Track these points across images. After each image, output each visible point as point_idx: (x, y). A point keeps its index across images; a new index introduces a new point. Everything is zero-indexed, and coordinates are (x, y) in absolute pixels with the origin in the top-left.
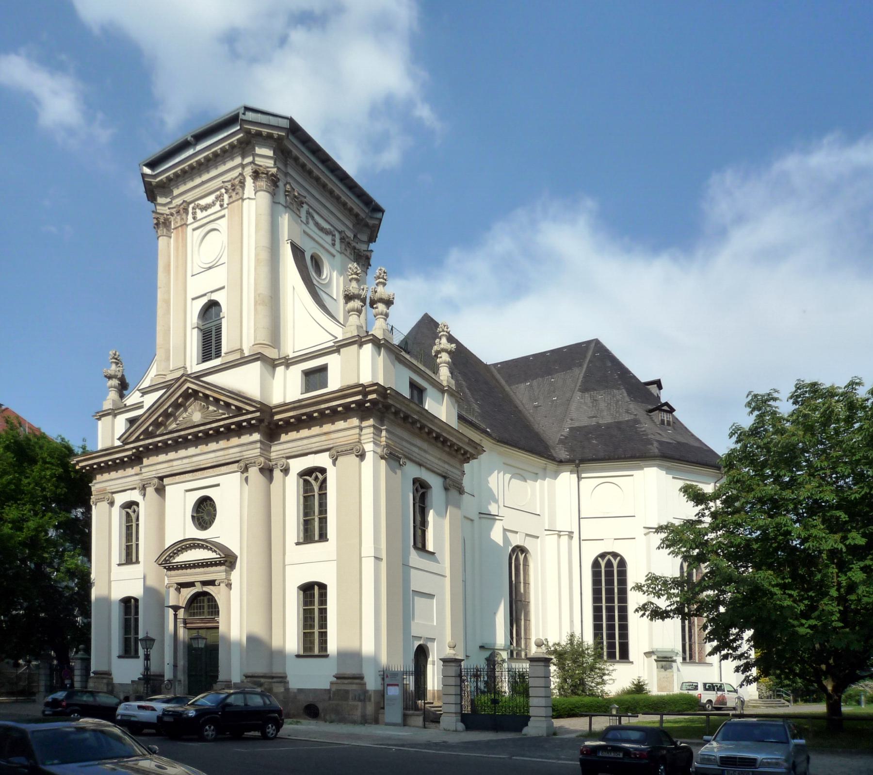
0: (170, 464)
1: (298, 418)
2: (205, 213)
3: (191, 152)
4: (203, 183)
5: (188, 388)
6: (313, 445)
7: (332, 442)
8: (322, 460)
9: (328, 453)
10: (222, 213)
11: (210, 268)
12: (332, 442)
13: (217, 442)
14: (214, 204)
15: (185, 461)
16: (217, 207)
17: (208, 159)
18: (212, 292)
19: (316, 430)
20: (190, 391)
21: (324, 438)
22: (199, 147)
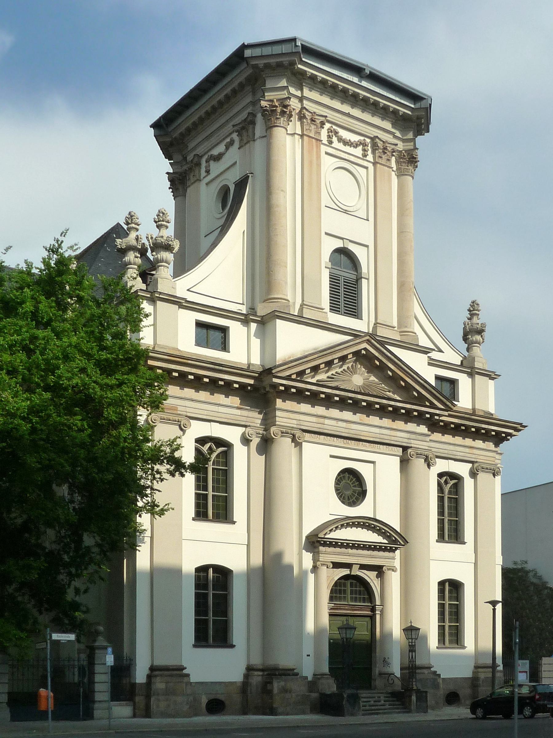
0: (321, 420)
1: (458, 426)
2: (341, 146)
3: (355, 80)
4: (348, 115)
5: (365, 349)
6: (458, 453)
7: (474, 456)
8: (463, 469)
9: (470, 465)
10: (365, 164)
11: (346, 212)
12: (474, 456)
13: (381, 418)
14: (355, 145)
15: (341, 424)
16: (359, 151)
17: (365, 100)
18: (351, 241)
19: (468, 442)
20: (363, 352)
21: (467, 450)
22: (364, 83)
